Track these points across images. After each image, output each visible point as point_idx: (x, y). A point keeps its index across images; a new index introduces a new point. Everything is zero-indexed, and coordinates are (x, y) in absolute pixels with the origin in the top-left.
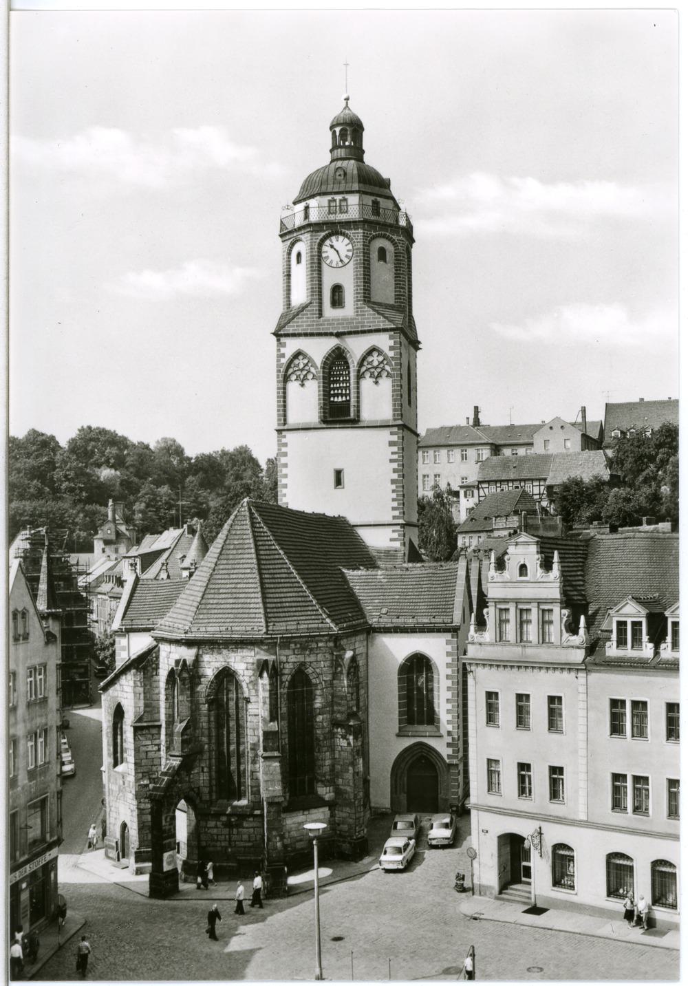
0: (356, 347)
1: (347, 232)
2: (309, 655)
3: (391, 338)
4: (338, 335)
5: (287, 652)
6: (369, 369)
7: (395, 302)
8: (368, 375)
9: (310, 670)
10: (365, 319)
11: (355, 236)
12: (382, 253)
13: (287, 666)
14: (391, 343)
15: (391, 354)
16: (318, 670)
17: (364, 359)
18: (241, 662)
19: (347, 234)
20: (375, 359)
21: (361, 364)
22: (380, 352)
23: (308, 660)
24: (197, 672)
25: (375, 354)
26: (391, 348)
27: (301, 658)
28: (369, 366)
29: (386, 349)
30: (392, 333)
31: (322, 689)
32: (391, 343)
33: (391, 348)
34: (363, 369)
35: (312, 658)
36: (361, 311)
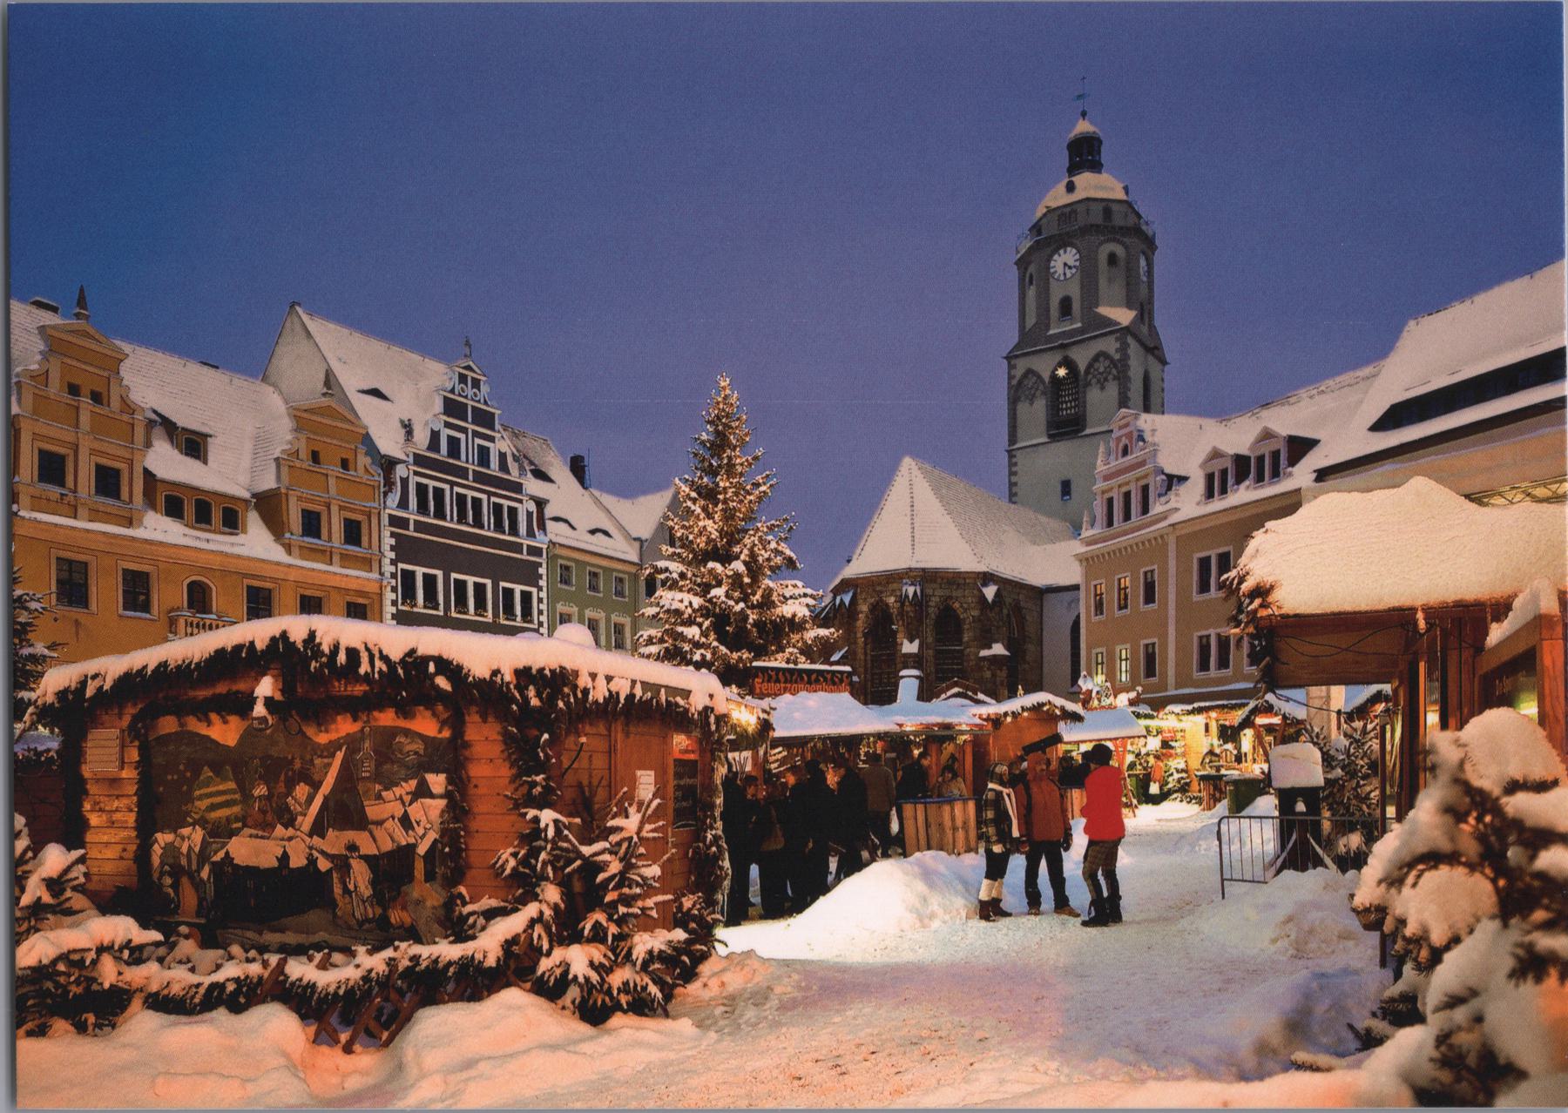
0: (1082, 357)
2: (956, 590)
4: (1063, 346)
5: (935, 586)
9: (957, 605)
13: (933, 599)
15: (1117, 357)
16: (965, 605)
17: (1090, 366)
18: (891, 595)
20: (1101, 366)
21: (1087, 371)
23: (954, 594)
24: (856, 609)
25: (1101, 359)
27: (947, 593)
31: (970, 623)
32: (1118, 345)
34: (1090, 377)
35: (958, 593)
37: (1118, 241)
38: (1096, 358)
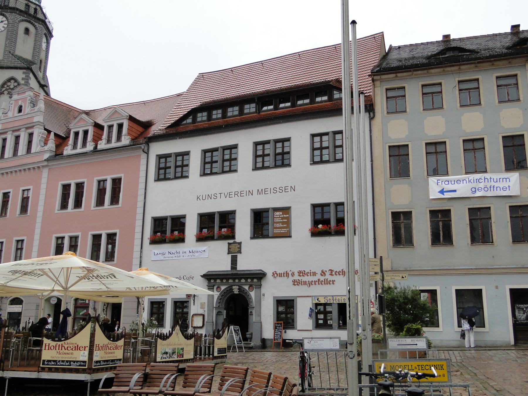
1: (5, 13)
3: (24, 73)
6: (8, 89)
7: (32, 59)
8: (6, 92)
10: (10, 61)
11: (10, 16)
12: (27, 31)
14: (24, 76)
19: (5, 15)
20: (12, 84)
22: (16, 81)
25: (12, 81)
26: (23, 79)
28: (8, 88)
29: (19, 79)
30: (25, 71)
33: (23, 79)
36: (7, 57)
37: (32, 23)
38: (9, 80)
